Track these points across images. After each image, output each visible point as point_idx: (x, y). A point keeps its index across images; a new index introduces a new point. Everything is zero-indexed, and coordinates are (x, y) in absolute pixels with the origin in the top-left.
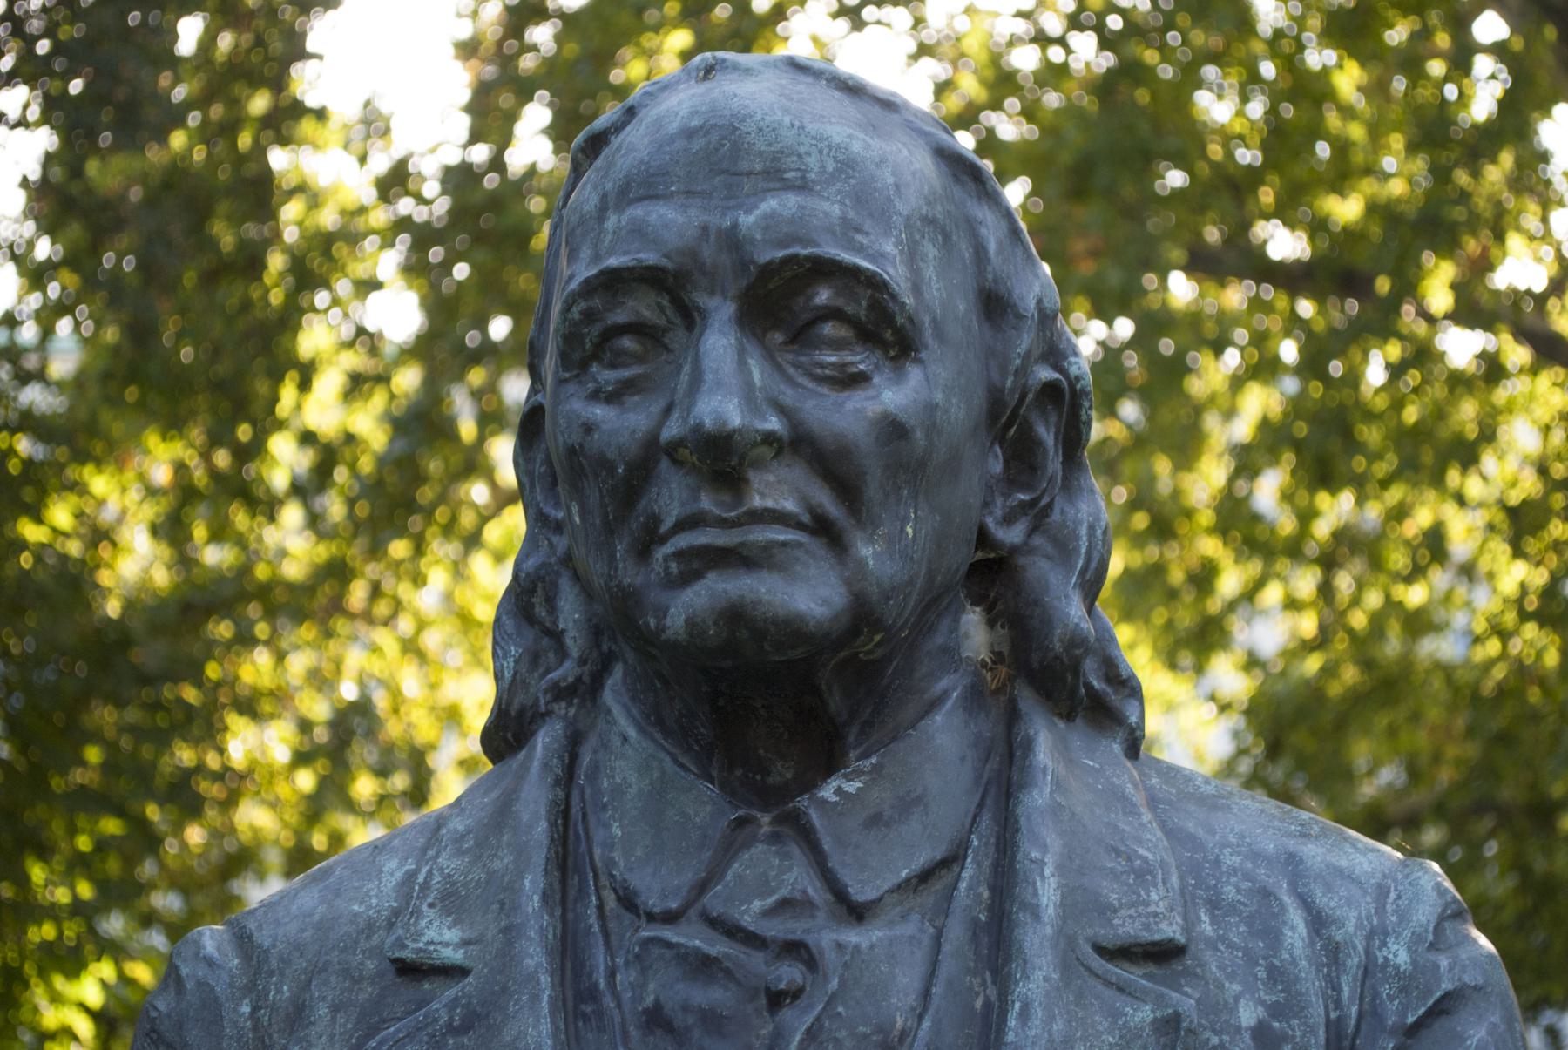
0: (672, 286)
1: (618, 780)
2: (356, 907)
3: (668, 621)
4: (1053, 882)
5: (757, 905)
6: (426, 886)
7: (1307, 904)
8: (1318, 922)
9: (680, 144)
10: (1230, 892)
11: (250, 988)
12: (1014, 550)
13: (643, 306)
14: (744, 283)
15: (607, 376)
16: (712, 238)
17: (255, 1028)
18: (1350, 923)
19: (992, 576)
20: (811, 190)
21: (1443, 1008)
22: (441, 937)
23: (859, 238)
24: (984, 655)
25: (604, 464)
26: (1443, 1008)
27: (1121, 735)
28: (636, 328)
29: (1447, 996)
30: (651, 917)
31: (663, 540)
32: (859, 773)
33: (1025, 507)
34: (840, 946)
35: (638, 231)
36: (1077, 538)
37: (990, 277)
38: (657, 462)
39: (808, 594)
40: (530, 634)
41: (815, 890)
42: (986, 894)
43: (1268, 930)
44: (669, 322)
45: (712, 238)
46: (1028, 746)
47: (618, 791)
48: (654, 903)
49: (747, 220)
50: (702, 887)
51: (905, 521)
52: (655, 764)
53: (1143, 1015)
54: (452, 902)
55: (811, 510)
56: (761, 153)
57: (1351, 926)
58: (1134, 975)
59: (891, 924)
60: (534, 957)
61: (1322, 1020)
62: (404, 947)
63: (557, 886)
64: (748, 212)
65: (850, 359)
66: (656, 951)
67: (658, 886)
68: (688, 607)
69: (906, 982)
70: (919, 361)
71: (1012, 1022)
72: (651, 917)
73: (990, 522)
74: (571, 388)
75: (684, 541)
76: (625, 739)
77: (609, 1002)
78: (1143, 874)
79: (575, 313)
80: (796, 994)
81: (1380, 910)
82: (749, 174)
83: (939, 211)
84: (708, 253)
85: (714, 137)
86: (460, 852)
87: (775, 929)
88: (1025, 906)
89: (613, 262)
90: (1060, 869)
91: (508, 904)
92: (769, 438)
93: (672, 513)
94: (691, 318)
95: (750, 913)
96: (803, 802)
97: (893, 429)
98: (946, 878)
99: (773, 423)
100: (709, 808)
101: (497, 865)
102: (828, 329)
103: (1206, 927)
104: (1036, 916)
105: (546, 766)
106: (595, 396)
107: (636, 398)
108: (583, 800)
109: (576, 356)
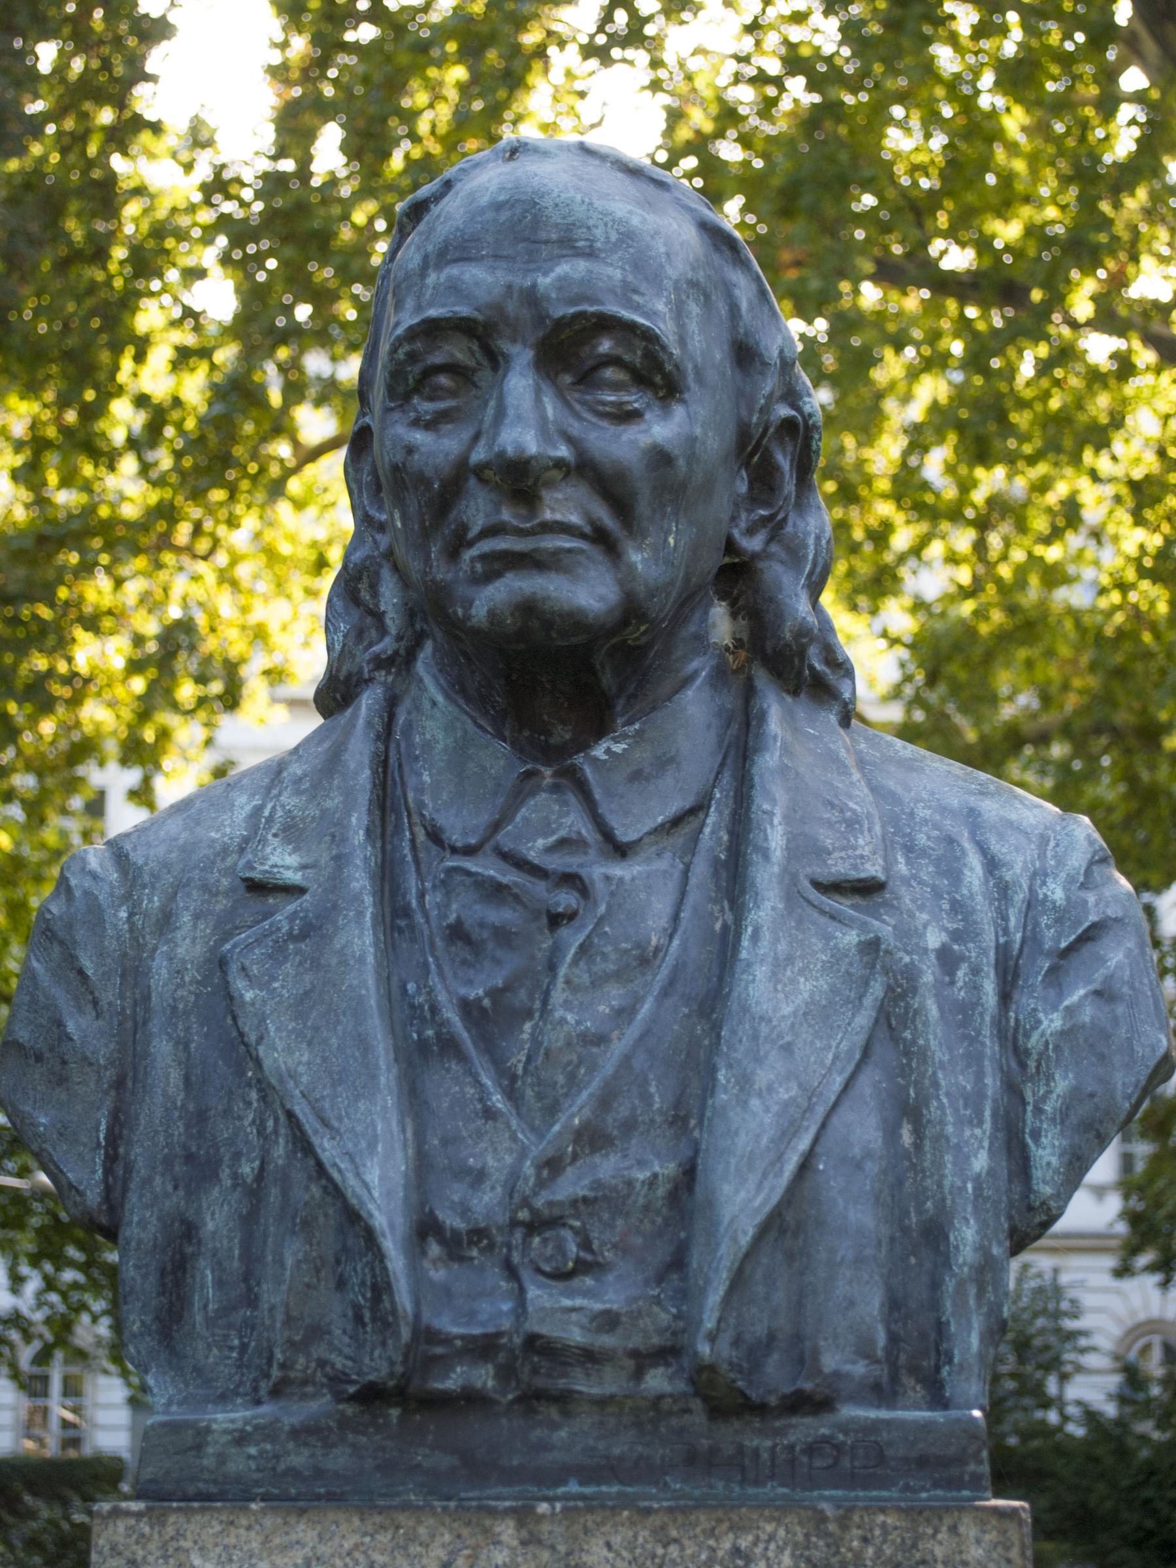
0: (482, 334)
1: (428, 736)
2: (213, 834)
3: (473, 612)
4: (780, 829)
5: (541, 843)
6: (270, 819)
7: (983, 849)
8: (992, 865)
9: (489, 215)
10: (922, 839)
11: (127, 897)
12: (755, 556)
13: (457, 350)
14: (541, 334)
15: (427, 407)
16: (515, 295)
17: (131, 930)
18: (1017, 867)
19: (736, 577)
20: (597, 257)
21: (1090, 935)
22: (283, 861)
23: (636, 298)
24: (728, 641)
25: (422, 480)
26: (1090, 935)
27: (837, 708)
28: (451, 368)
29: (1094, 926)
30: (454, 850)
31: (470, 544)
32: (625, 736)
33: (765, 521)
34: (607, 878)
35: (454, 288)
36: (806, 547)
37: (742, 331)
38: (467, 480)
39: (589, 592)
40: (356, 614)
41: (587, 831)
42: (726, 838)
43: (952, 871)
44: (478, 363)
45: (515, 295)
46: (762, 717)
47: (428, 746)
48: (456, 837)
49: (544, 281)
50: (496, 826)
51: (667, 533)
52: (458, 725)
53: (850, 938)
54: (292, 833)
55: (592, 522)
56: (557, 225)
57: (1018, 868)
58: (843, 905)
59: (648, 860)
60: (360, 880)
61: (993, 944)
62: (254, 869)
63: (378, 822)
64: (545, 274)
65: (626, 398)
66: (459, 878)
67: (460, 825)
68: (489, 601)
69: (659, 908)
70: (683, 401)
71: (745, 943)
72: (454, 850)
73: (736, 533)
74: (396, 415)
75: (486, 546)
76: (434, 704)
77: (419, 919)
78: (853, 823)
79: (401, 354)
80: (571, 916)
81: (1042, 856)
82: (546, 242)
83: (701, 276)
84: (511, 307)
85: (518, 211)
86: (298, 793)
87: (556, 863)
88: (757, 849)
89: (433, 313)
90: (788, 820)
91: (338, 838)
92: (559, 464)
93: (478, 523)
94: (496, 361)
95: (535, 849)
96: (579, 759)
97: (660, 458)
98: (694, 823)
99: (563, 451)
100: (502, 762)
101: (329, 804)
102: (609, 373)
103: (902, 867)
104: (766, 856)
105: (369, 724)
106: (416, 423)
107: (450, 426)
108: (399, 752)
109: (401, 389)
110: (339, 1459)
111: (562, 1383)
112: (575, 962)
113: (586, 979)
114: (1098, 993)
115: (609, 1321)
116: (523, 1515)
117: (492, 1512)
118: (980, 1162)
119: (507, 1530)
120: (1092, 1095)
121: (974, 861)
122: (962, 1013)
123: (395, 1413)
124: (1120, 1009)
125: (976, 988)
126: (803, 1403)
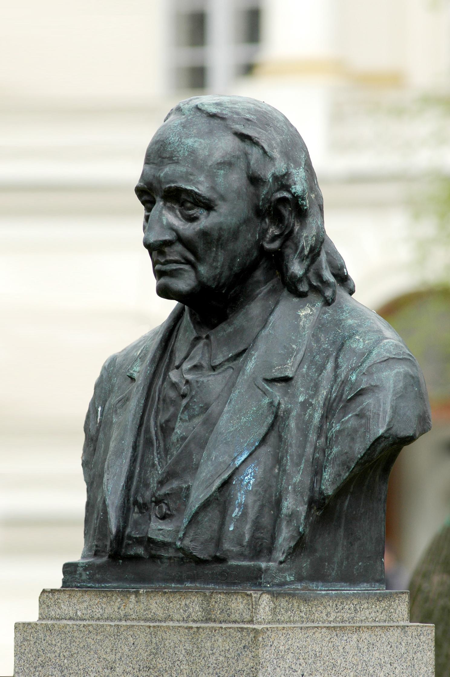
21: (361, 393)
23: (191, 177)
26: (361, 393)
29: (362, 390)
63: (158, 356)
111: (159, 553)
112: (183, 412)
113: (187, 418)
114: (357, 415)
116: (137, 593)
117: (129, 592)
119: (133, 598)
120: (346, 453)
123: (121, 561)
124: (363, 421)
125: (311, 416)
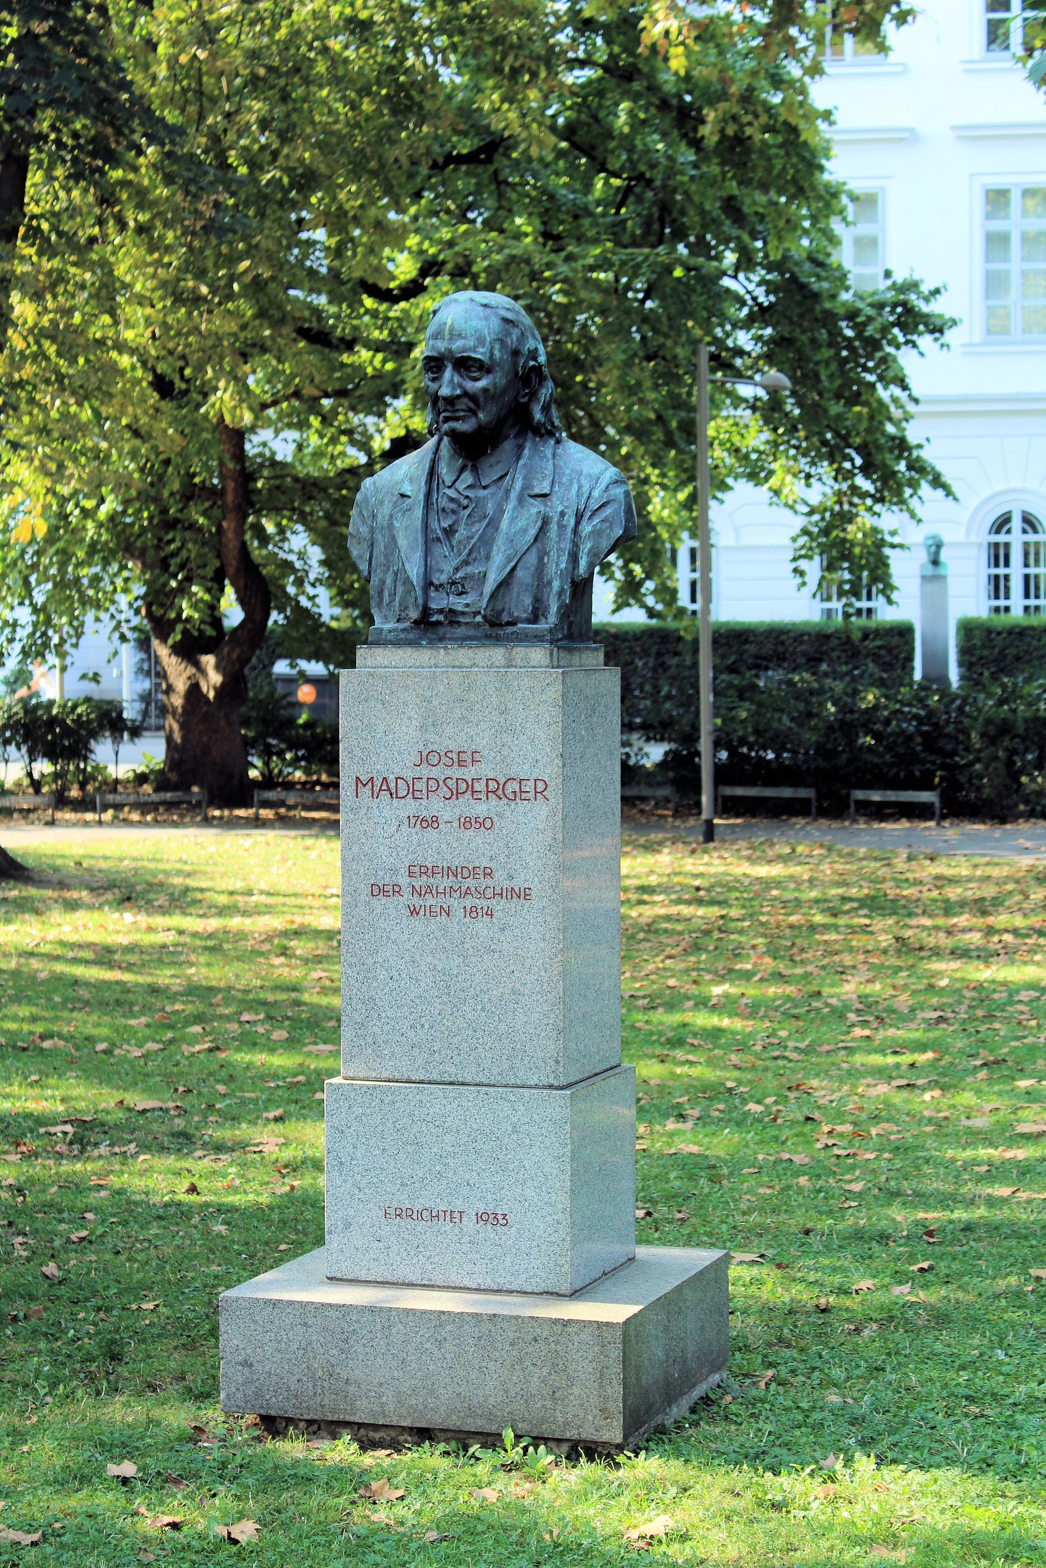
53: (534, 511)
97: (485, 390)
99: (458, 392)
110: (411, 636)
115: (467, 605)
118: (563, 566)
121: (575, 487)
122: (561, 527)
126: (510, 624)
